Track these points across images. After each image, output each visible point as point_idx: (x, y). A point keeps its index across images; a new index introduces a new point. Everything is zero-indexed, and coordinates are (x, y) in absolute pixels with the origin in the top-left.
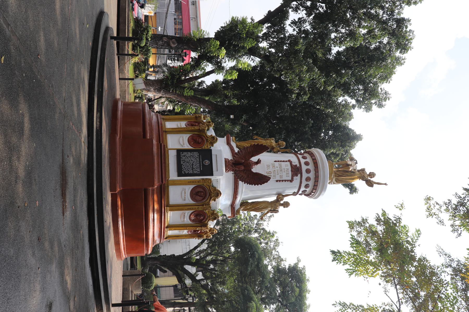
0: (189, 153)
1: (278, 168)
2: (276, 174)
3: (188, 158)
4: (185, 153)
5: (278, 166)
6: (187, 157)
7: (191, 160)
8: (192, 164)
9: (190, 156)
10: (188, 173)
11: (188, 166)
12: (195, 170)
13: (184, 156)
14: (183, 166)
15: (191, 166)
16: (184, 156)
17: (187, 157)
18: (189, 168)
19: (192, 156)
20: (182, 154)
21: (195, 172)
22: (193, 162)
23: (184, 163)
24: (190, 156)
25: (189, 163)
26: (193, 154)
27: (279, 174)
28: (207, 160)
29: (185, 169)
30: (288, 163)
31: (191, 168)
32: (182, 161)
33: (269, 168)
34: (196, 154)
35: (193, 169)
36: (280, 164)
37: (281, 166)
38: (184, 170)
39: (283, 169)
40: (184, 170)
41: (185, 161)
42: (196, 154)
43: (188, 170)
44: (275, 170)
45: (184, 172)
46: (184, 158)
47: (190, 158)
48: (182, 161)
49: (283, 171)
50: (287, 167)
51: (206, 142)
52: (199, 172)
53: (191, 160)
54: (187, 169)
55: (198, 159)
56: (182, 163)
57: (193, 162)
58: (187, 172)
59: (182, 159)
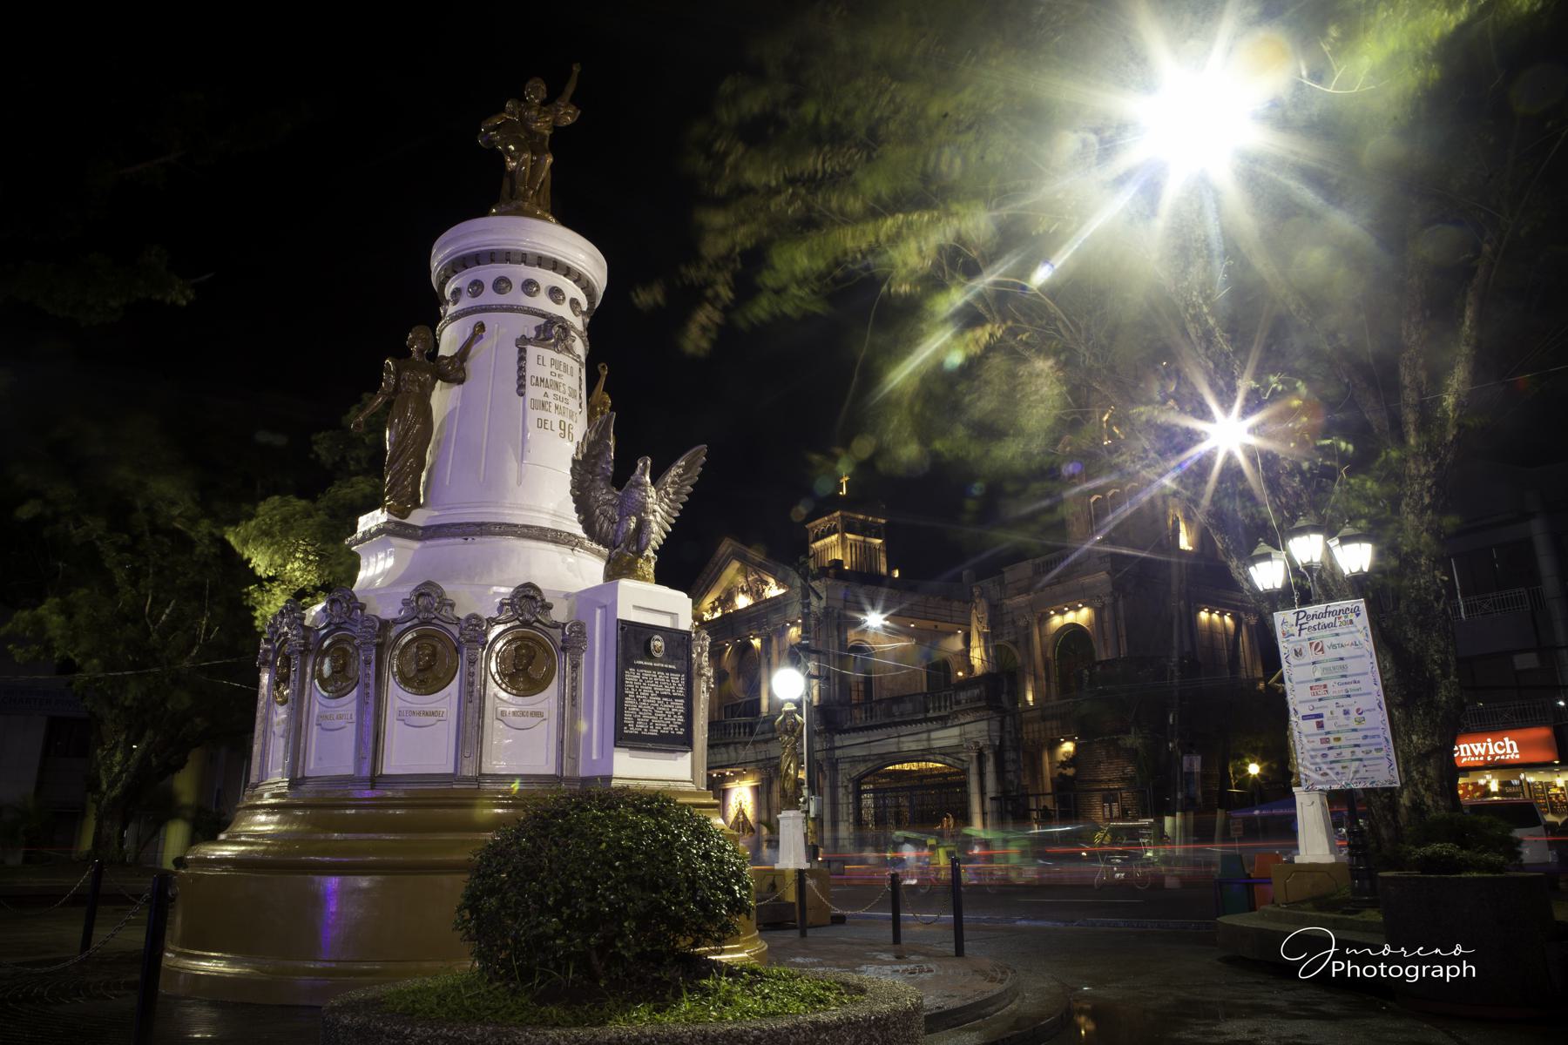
0: (628, 701)
1: (551, 392)
2: (566, 406)
3: (641, 709)
4: (628, 719)
5: (543, 390)
6: (638, 713)
7: (648, 697)
8: (659, 695)
9: (637, 699)
10: (682, 714)
11: (664, 712)
12: (676, 690)
13: (635, 720)
14: (662, 727)
15: (665, 702)
16: (635, 720)
17: (638, 713)
18: (670, 709)
19: (635, 692)
20: (628, 729)
21: (681, 691)
22: (655, 692)
23: (654, 724)
24: (637, 699)
25: (655, 707)
26: (630, 688)
27: (566, 396)
28: (652, 645)
29: (672, 722)
30: (532, 351)
31: (669, 703)
32: (649, 729)
33: (549, 422)
34: (631, 677)
35: (673, 698)
36: (534, 380)
37: (542, 381)
38: (674, 728)
39: (553, 378)
40: (674, 728)
41: (650, 720)
42: (631, 677)
43: (676, 713)
44: (557, 408)
45: (680, 726)
46: (640, 725)
47: (642, 699)
48: (649, 729)
49: (556, 379)
50: (547, 362)
51: (535, 628)
52: (680, 678)
53: (648, 697)
54: (672, 715)
55: (647, 673)
56: (654, 733)
57: (655, 692)
58: (681, 719)
59: (643, 729)
